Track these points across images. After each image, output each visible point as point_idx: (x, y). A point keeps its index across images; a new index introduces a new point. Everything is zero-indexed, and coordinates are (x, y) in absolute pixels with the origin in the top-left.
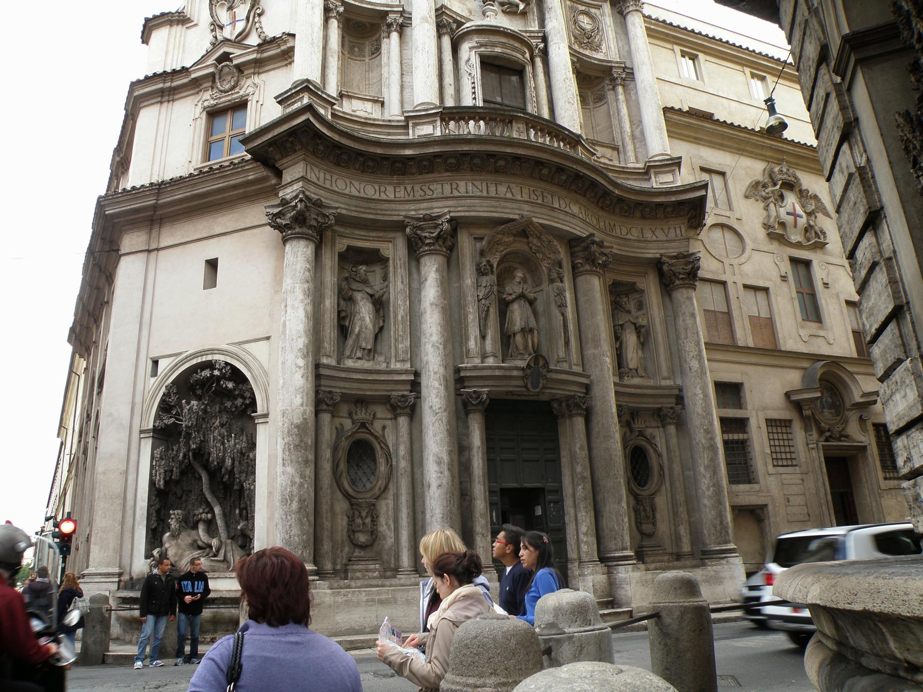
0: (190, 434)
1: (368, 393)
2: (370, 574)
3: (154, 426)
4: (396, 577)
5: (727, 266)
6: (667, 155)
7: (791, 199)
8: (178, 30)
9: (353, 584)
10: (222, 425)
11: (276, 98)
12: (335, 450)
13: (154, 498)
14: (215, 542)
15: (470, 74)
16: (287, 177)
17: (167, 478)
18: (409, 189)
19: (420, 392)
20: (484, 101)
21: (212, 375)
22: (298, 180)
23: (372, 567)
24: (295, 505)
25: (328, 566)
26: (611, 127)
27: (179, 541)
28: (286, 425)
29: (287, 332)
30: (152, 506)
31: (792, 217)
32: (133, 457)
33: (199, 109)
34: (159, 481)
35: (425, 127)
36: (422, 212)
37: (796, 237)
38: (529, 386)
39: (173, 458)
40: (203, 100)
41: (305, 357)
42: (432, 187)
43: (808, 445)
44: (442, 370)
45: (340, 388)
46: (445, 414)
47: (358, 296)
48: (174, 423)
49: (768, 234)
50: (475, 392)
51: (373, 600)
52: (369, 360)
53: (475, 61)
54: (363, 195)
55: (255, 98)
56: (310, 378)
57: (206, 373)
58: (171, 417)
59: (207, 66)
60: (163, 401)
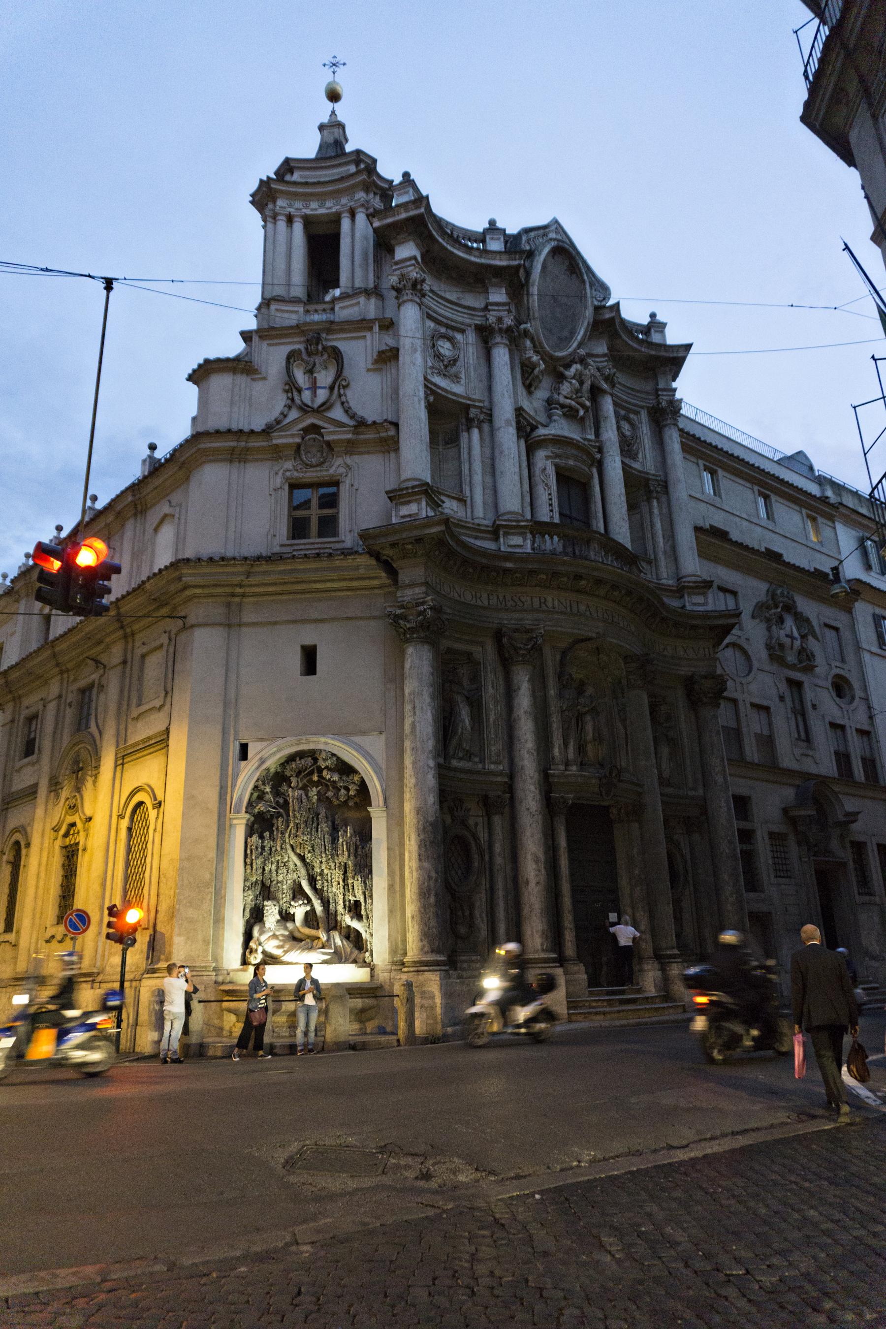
5: (738, 684)
6: (698, 576)
7: (789, 622)
8: (242, 380)
11: (387, 492)
15: (546, 485)
16: (404, 577)
18: (501, 598)
20: (561, 514)
22: (422, 584)
24: (432, 900)
26: (644, 538)
31: (790, 640)
33: (279, 480)
35: (516, 538)
36: (513, 622)
37: (791, 658)
38: (604, 794)
40: (285, 467)
42: (523, 599)
43: (800, 859)
44: (536, 775)
46: (540, 817)
47: (459, 699)
49: (770, 655)
50: (562, 797)
53: (551, 471)
54: (463, 600)
55: (348, 481)
59: (293, 436)
60: (256, 788)
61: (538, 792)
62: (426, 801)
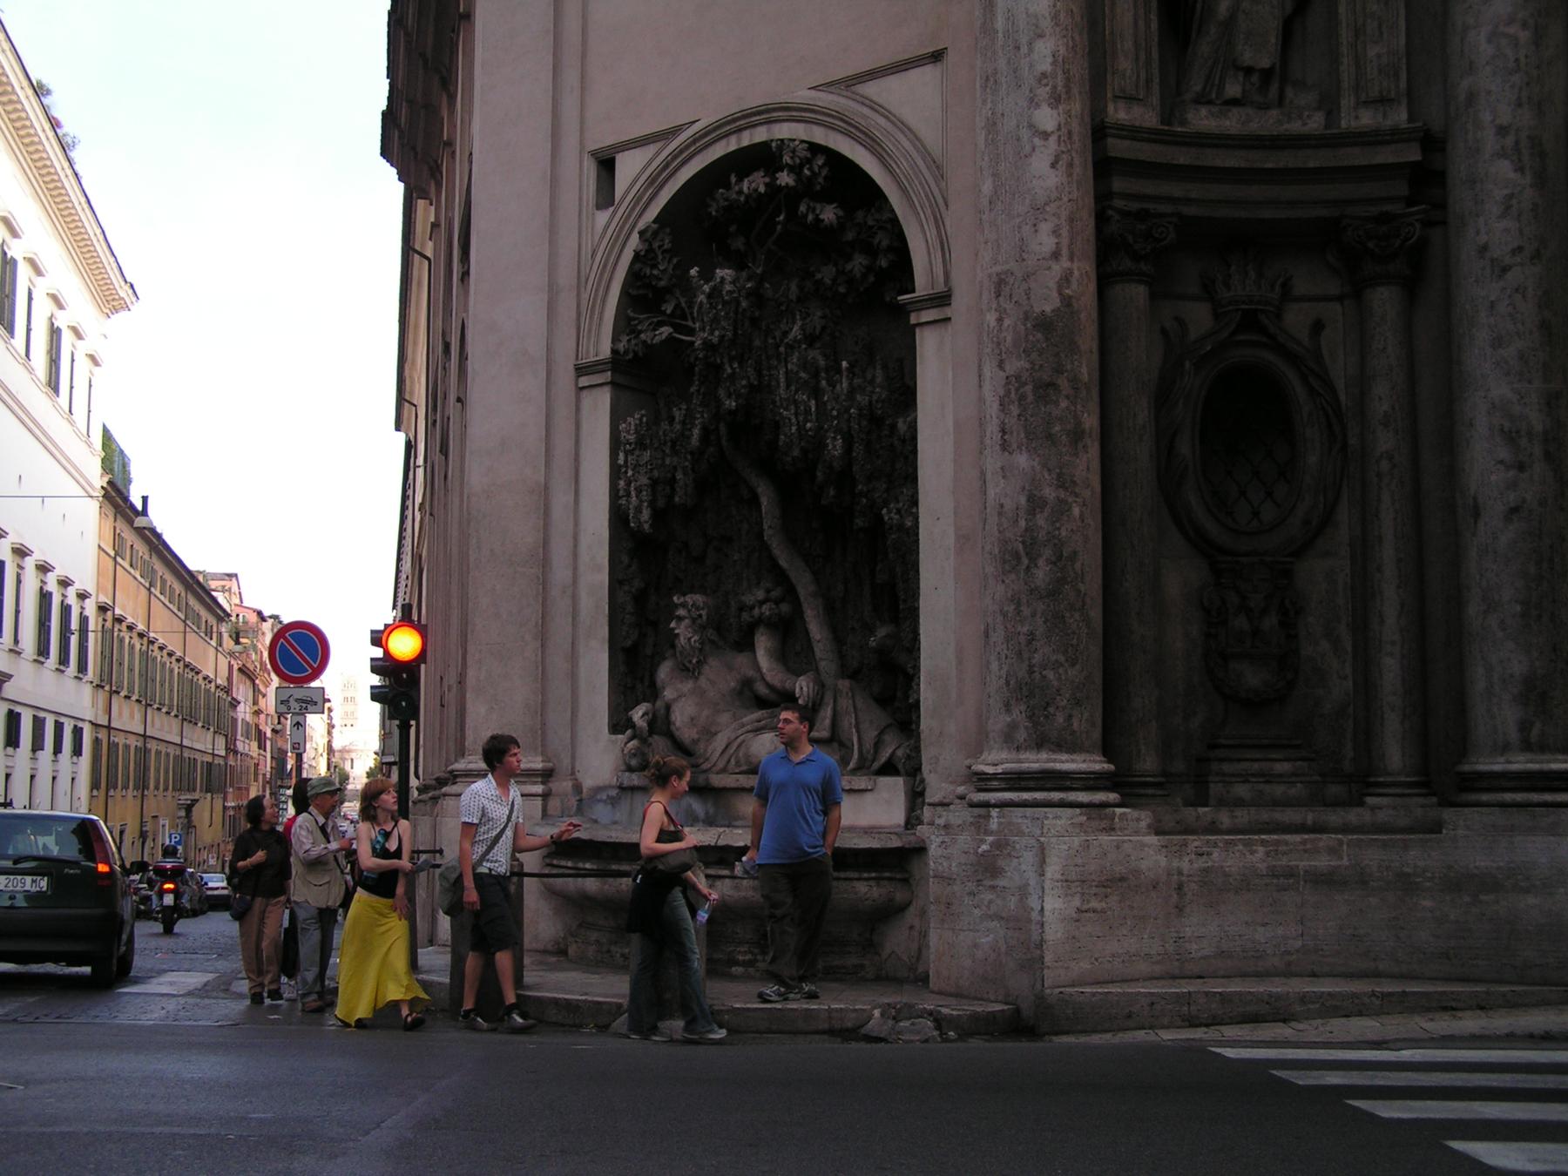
0: (719, 368)
1: (1267, 214)
2: (1278, 790)
3: (614, 351)
4: (1361, 804)
9: (1225, 819)
10: (811, 339)
12: (1163, 397)
13: (625, 559)
14: (803, 687)
17: (661, 503)
19: (1442, 206)
21: (773, 188)
23: (1282, 767)
25: (1148, 763)
27: (703, 681)
28: (1007, 322)
29: (1000, 24)
30: (621, 583)
32: (563, 445)
34: (639, 510)
39: (674, 443)
41: (1055, 100)
45: (1170, 200)
48: (670, 338)
51: (1291, 873)
52: (1264, 107)
56: (1077, 170)
57: (756, 182)
58: (660, 324)
60: (634, 276)
61: (1528, 180)
62: (1022, 248)
